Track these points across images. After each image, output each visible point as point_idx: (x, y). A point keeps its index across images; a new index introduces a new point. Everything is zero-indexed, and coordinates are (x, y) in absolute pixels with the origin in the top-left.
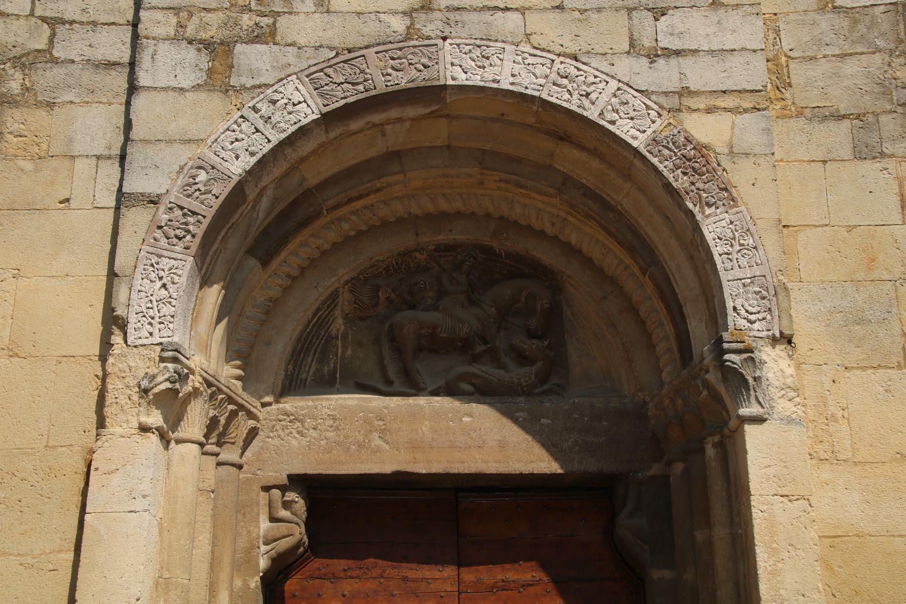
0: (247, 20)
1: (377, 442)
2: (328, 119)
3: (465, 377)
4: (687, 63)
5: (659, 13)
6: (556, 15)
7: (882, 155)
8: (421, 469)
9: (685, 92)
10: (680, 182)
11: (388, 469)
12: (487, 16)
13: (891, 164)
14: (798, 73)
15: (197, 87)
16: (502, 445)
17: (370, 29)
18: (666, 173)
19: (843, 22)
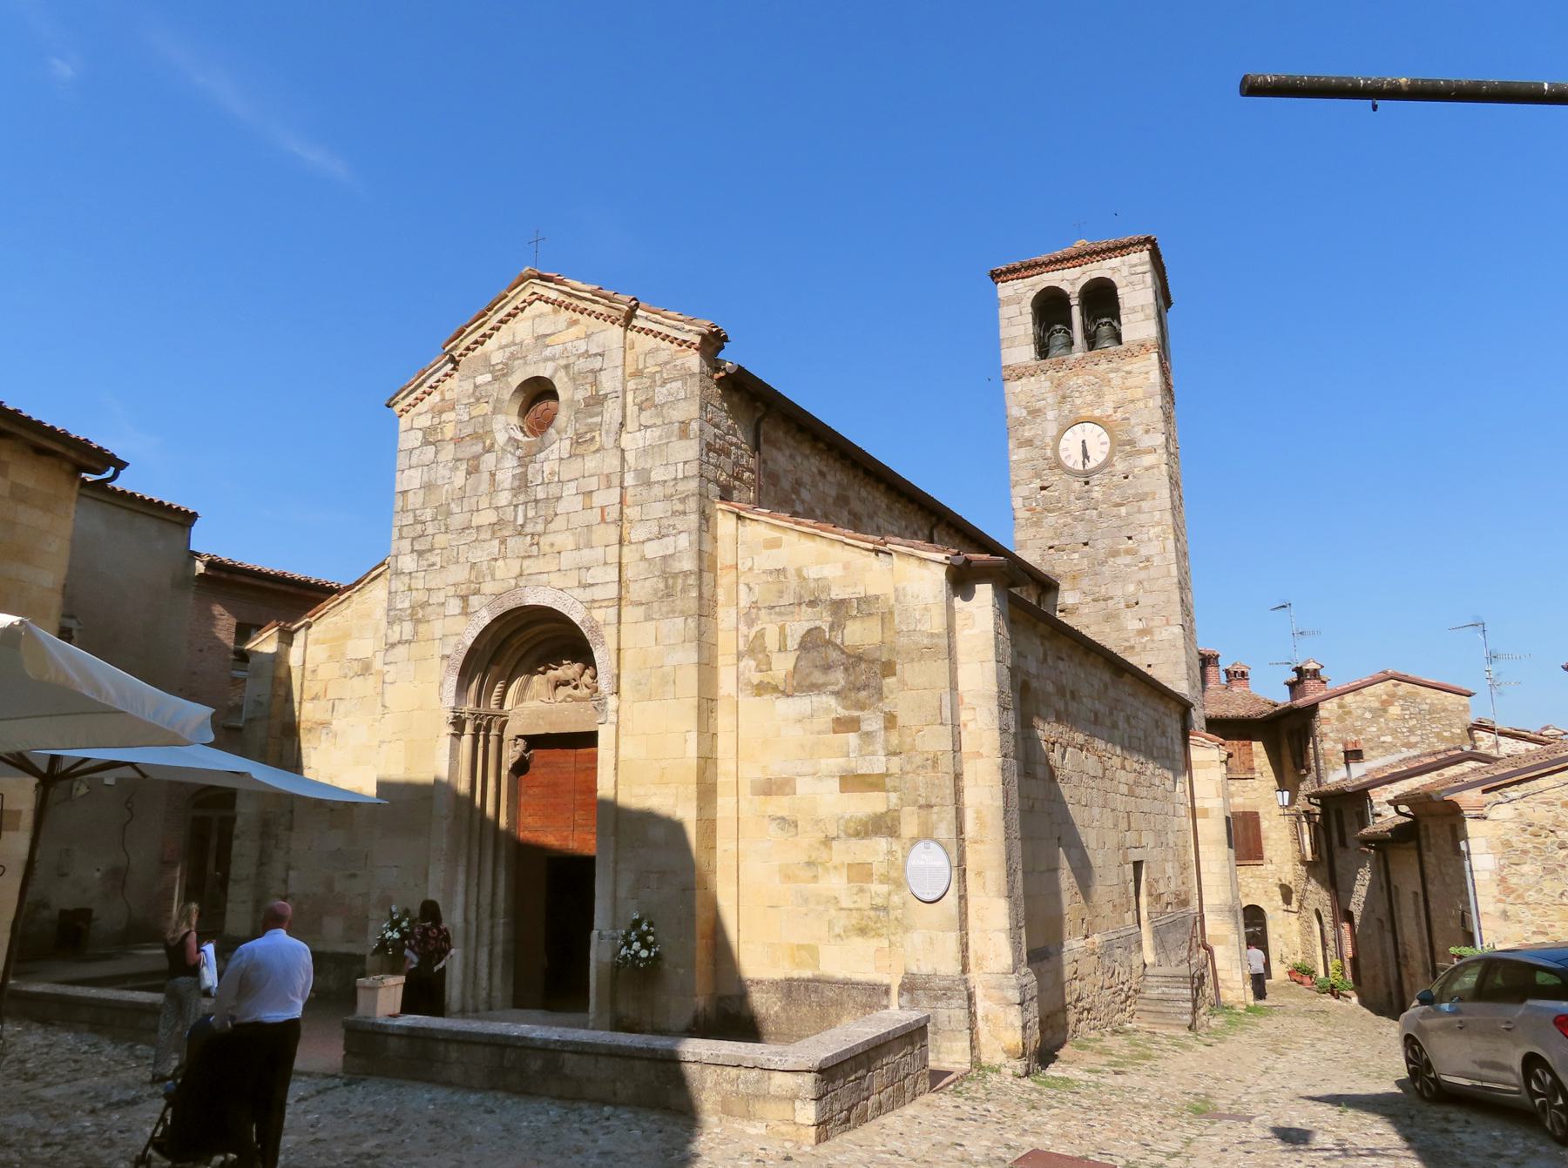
0: (473, 586)
1: (541, 722)
2: (494, 621)
3: (569, 696)
4: (594, 588)
5: (588, 569)
6: (557, 574)
7: (653, 619)
8: (553, 732)
9: (594, 601)
10: (588, 636)
11: (542, 732)
12: (538, 576)
13: (654, 622)
14: (632, 587)
15: (460, 614)
16: (576, 721)
17: (505, 585)
18: (584, 631)
19: (644, 565)
